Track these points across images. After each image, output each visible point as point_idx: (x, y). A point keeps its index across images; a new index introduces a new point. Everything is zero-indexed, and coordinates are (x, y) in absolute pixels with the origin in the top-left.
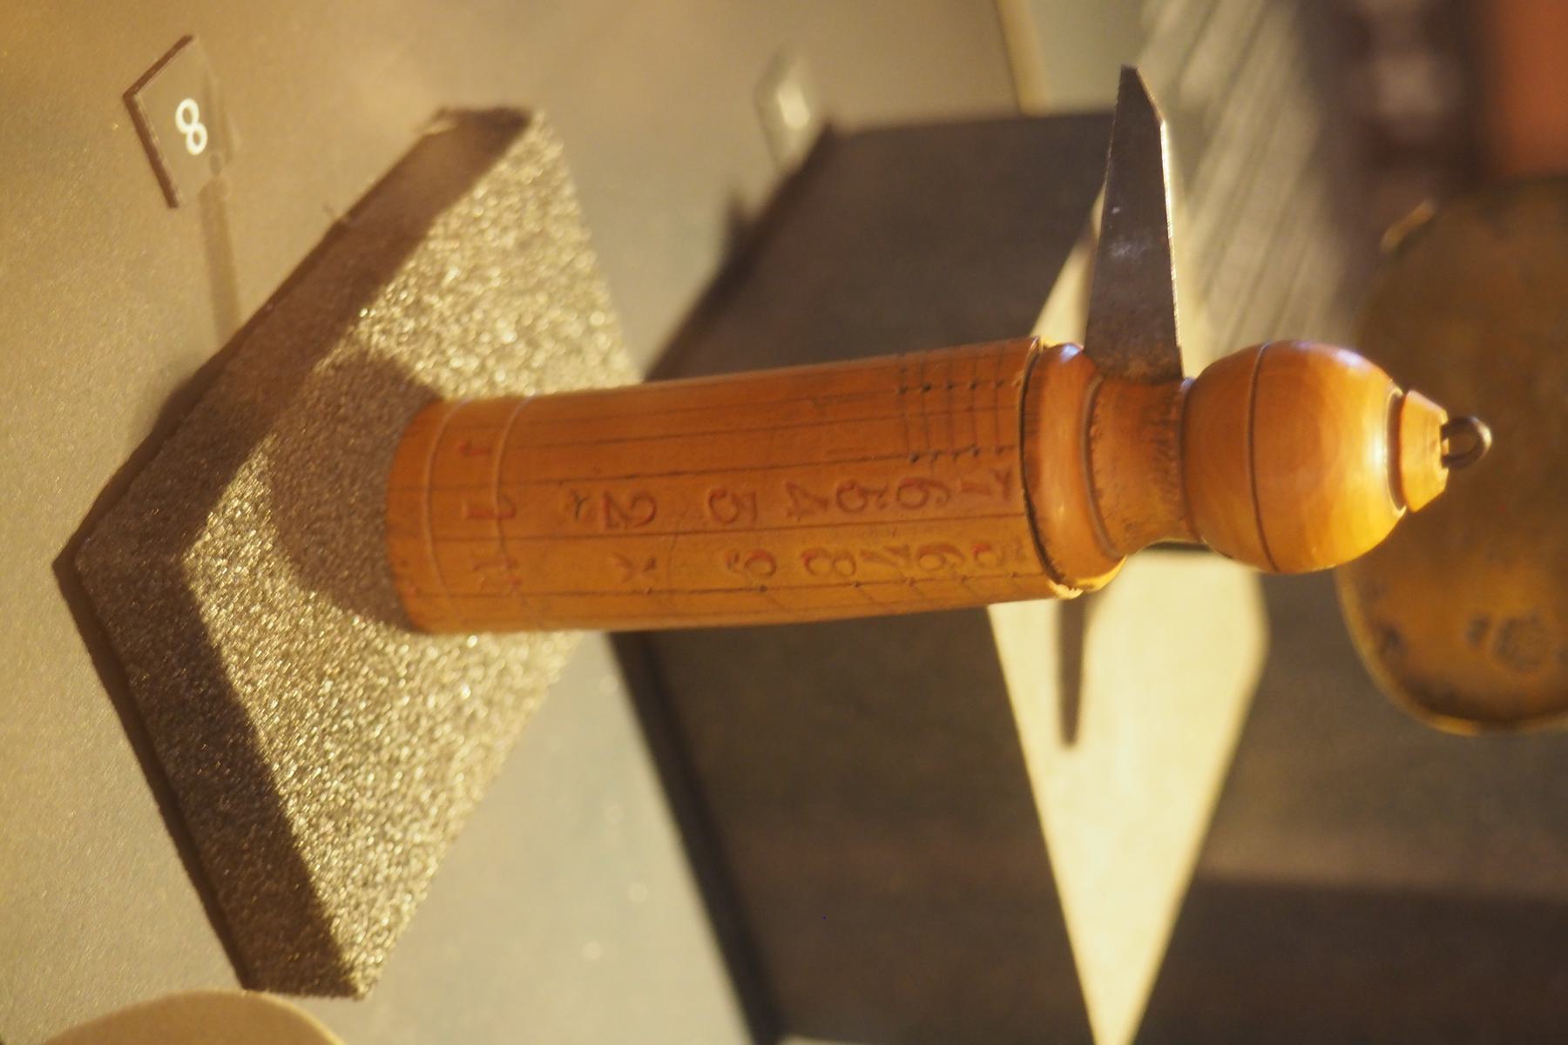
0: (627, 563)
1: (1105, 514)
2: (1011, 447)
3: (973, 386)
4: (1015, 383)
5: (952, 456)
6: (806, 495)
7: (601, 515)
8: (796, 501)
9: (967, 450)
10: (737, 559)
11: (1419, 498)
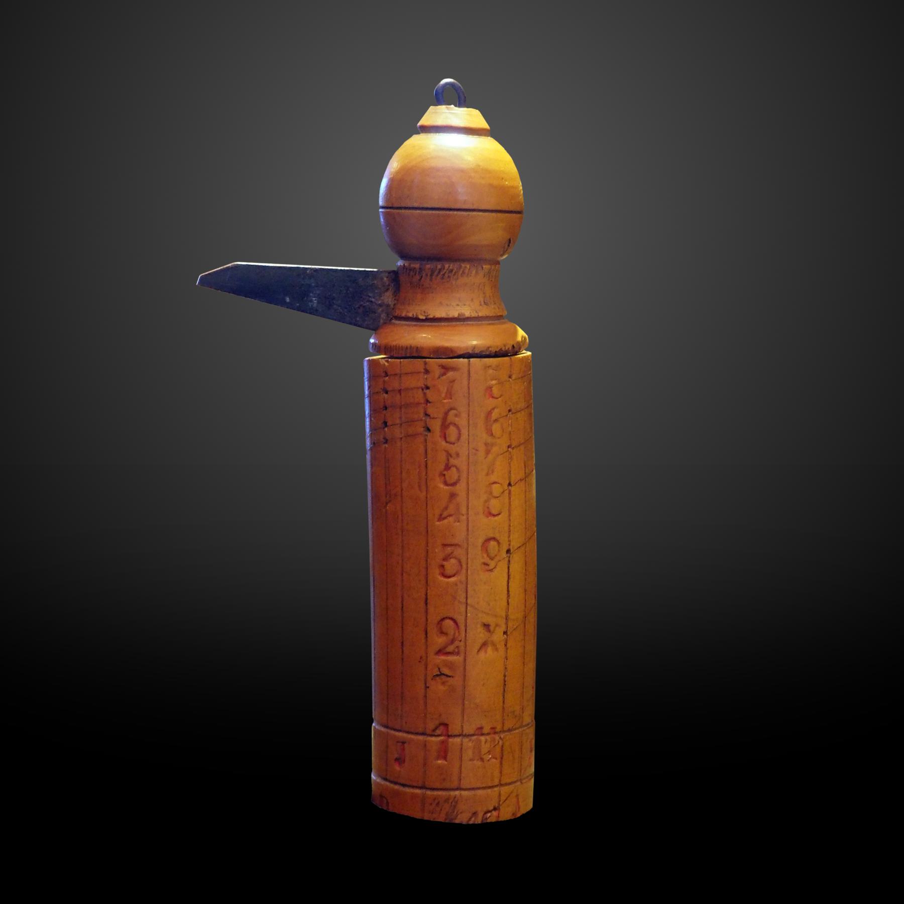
0: (484, 644)
1: (474, 315)
2: (426, 363)
3: (387, 392)
4: (386, 364)
5: (429, 404)
6: (446, 508)
7: (450, 658)
8: (450, 515)
9: (425, 394)
10: (486, 564)
11: (482, 123)
